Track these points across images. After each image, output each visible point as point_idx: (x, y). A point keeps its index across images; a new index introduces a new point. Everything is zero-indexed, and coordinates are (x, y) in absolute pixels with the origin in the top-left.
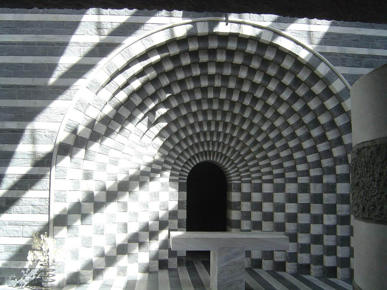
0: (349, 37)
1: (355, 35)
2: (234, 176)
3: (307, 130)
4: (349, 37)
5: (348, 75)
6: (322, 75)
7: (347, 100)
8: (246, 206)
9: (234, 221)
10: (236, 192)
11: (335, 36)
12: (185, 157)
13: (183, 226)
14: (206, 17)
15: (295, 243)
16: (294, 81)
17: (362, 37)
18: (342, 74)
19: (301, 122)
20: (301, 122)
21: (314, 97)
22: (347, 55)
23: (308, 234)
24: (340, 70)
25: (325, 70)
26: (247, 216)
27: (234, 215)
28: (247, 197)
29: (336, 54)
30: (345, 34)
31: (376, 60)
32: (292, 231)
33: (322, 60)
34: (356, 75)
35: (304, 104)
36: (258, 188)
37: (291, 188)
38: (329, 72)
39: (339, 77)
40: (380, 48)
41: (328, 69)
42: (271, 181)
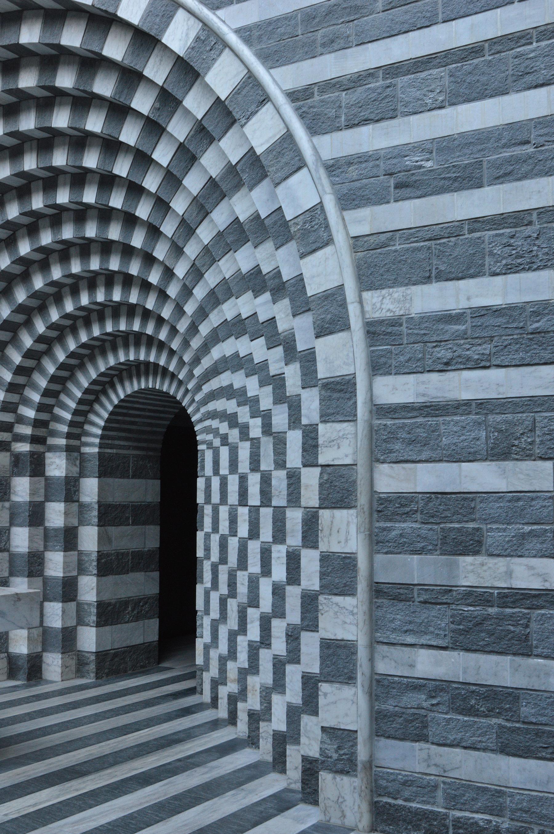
5: (258, 26)
7: (250, 123)
13: (90, 571)
18: (238, 31)
25: (187, 35)
34: (286, 18)
39: (226, 45)
41: (196, 27)
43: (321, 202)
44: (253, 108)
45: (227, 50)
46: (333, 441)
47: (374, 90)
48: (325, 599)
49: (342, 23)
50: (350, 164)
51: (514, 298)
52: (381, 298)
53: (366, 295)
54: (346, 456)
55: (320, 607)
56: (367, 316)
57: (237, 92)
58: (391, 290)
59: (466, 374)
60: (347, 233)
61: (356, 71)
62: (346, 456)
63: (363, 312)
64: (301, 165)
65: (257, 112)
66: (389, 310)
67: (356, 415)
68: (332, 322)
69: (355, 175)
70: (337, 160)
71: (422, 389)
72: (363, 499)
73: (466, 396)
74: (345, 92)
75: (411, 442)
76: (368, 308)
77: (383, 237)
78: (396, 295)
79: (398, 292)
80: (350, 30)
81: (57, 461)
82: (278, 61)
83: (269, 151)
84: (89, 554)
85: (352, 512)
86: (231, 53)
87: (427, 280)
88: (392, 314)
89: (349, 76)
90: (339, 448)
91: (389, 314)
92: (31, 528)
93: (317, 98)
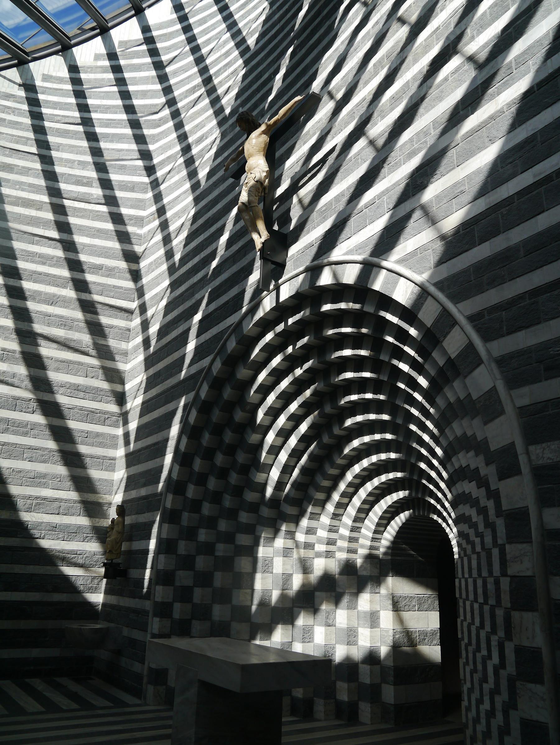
7: (446, 339)
25: (406, 291)
31: (504, 211)
43: (495, 386)
45: (430, 297)
46: (517, 557)
48: (521, 684)
49: (499, 268)
52: (542, 449)
53: (532, 448)
54: (528, 569)
55: (518, 692)
56: (534, 463)
57: (437, 321)
58: (549, 443)
60: (514, 406)
61: (511, 296)
62: (528, 569)
63: (530, 460)
64: (479, 362)
65: (450, 332)
66: (549, 458)
67: (531, 538)
70: (503, 356)
74: (505, 312)
76: (533, 457)
78: (553, 447)
82: (460, 298)
83: (459, 355)
85: (535, 614)
86: (432, 298)
88: (551, 461)
89: (506, 301)
90: (522, 563)
91: (549, 461)
92: (349, 611)
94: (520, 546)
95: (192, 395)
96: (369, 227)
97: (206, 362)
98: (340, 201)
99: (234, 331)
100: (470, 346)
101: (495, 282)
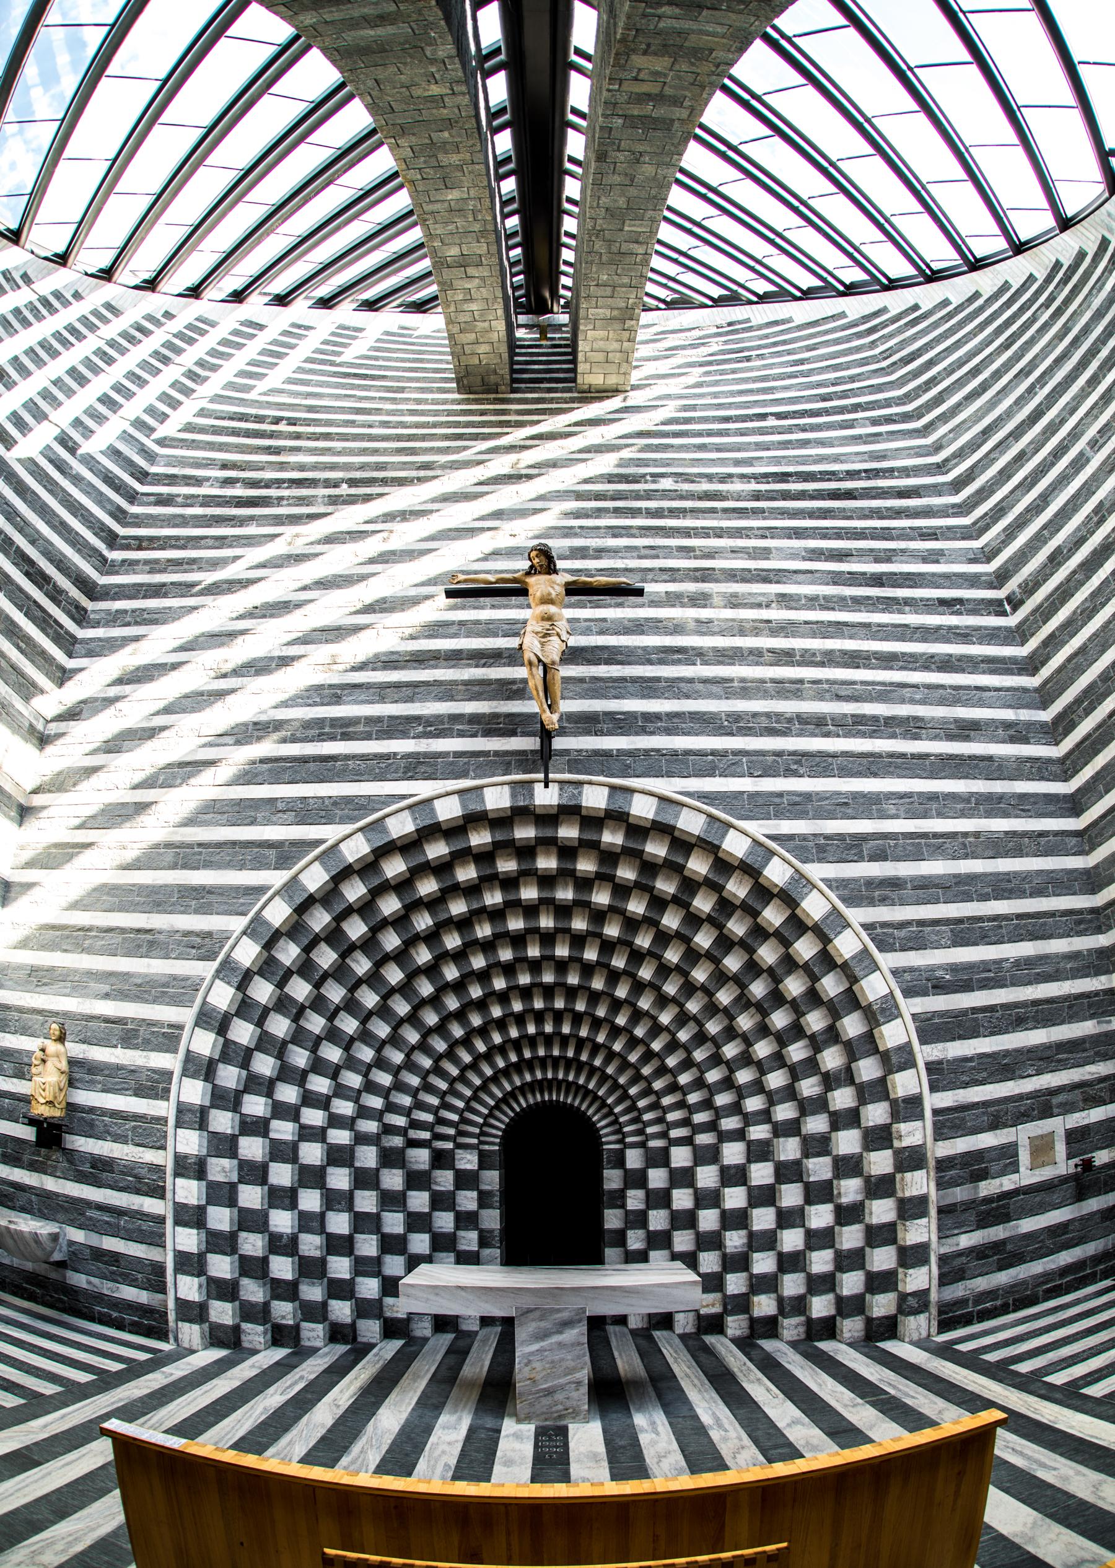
0: (827, 798)
1: (839, 793)
2: (607, 1135)
3: (758, 1018)
4: (827, 798)
5: (836, 880)
6: (777, 886)
8: (635, 1200)
9: (611, 1231)
10: (612, 1168)
11: (798, 799)
12: (492, 1095)
14: (504, 775)
15: (745, 1274)
16: (717, 907)
17: (856, 796)
18: (822, 880)
19: (744, 1001)
20: (744, 1001)
21: (765, 940)
22: (827, 837)
23: (771, 1253)
24: (816, 871)
26: (639, 1220)
27: (612, 1219)
28: (638, 1179)
29: (804, 838)
30: (817, 793)
31: (892, 843)
32: (736, 1247)
33: (772, 853)
35: (746, 957)
36: (661, 1159)
37: (733, 1153)
38: (792, 878)
39: (814, 887)
40: (896, 817)
41: (790, 872)
42: (688, 1141)
44: (839, 929)
47: (913, 932)
50: (905, 972)
51: (995, 1048)
59: (976, 1088)
68: (905, 1063)
69: (909, 978)
70: (897, 968)
71: (956, 1098)
72: (932, 1163)
73: (977, 1100)
75: (952, 1128)
77: (929, 1015)
79: (940, 1046)
80: (894, 895)
81: (469, 1157)
84: (491, 1231)
85: (924, 1171)
87: (953, 1039)
93: (879, 930)
94: (912, 1123)
95: (277, 878)
96: (718, 780)
97: (329, 833)
98: (652, 722)
99: (409, 807)
100: (865, 950)
101: (884, 901)
